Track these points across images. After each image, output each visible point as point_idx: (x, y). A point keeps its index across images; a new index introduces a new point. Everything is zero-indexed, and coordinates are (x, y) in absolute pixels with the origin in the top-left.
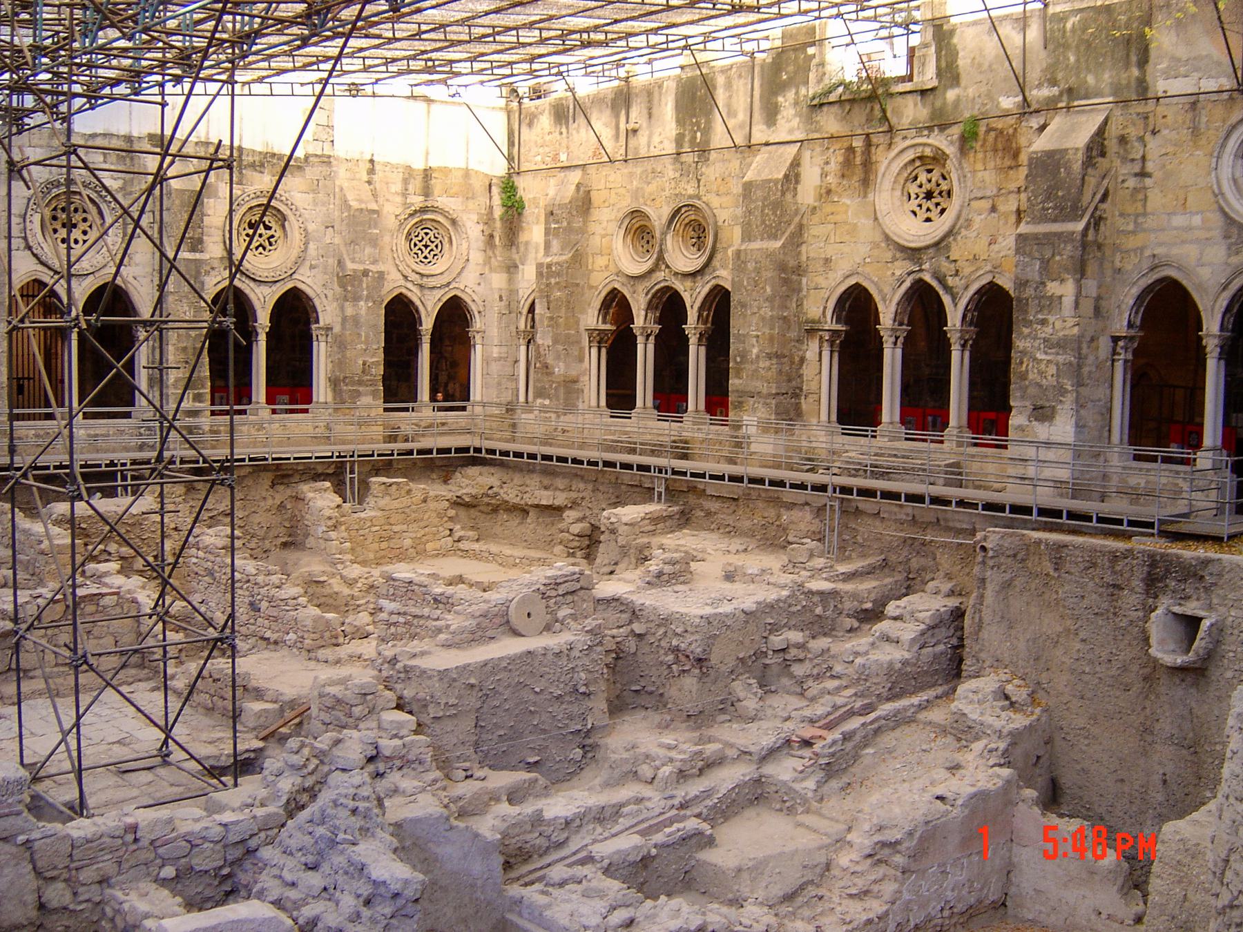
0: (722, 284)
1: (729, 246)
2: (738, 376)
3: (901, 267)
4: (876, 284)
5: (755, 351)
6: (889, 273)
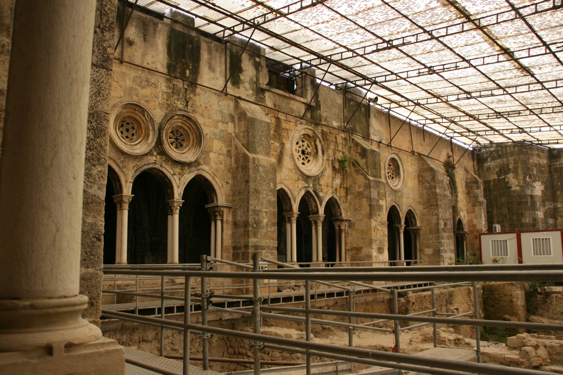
0: (204, 174)
1: (211, 151)
2: (255, 236)
3: (302, 184)
4: (290, 190)
5: (265, 221)
6: (296, 186)
